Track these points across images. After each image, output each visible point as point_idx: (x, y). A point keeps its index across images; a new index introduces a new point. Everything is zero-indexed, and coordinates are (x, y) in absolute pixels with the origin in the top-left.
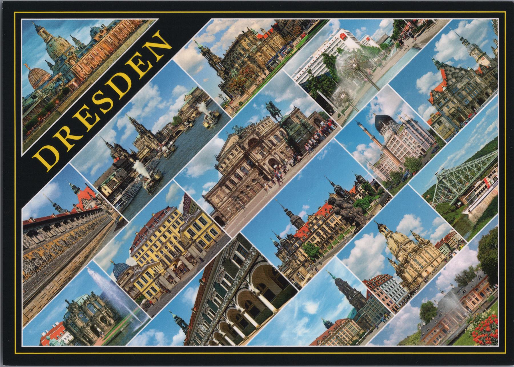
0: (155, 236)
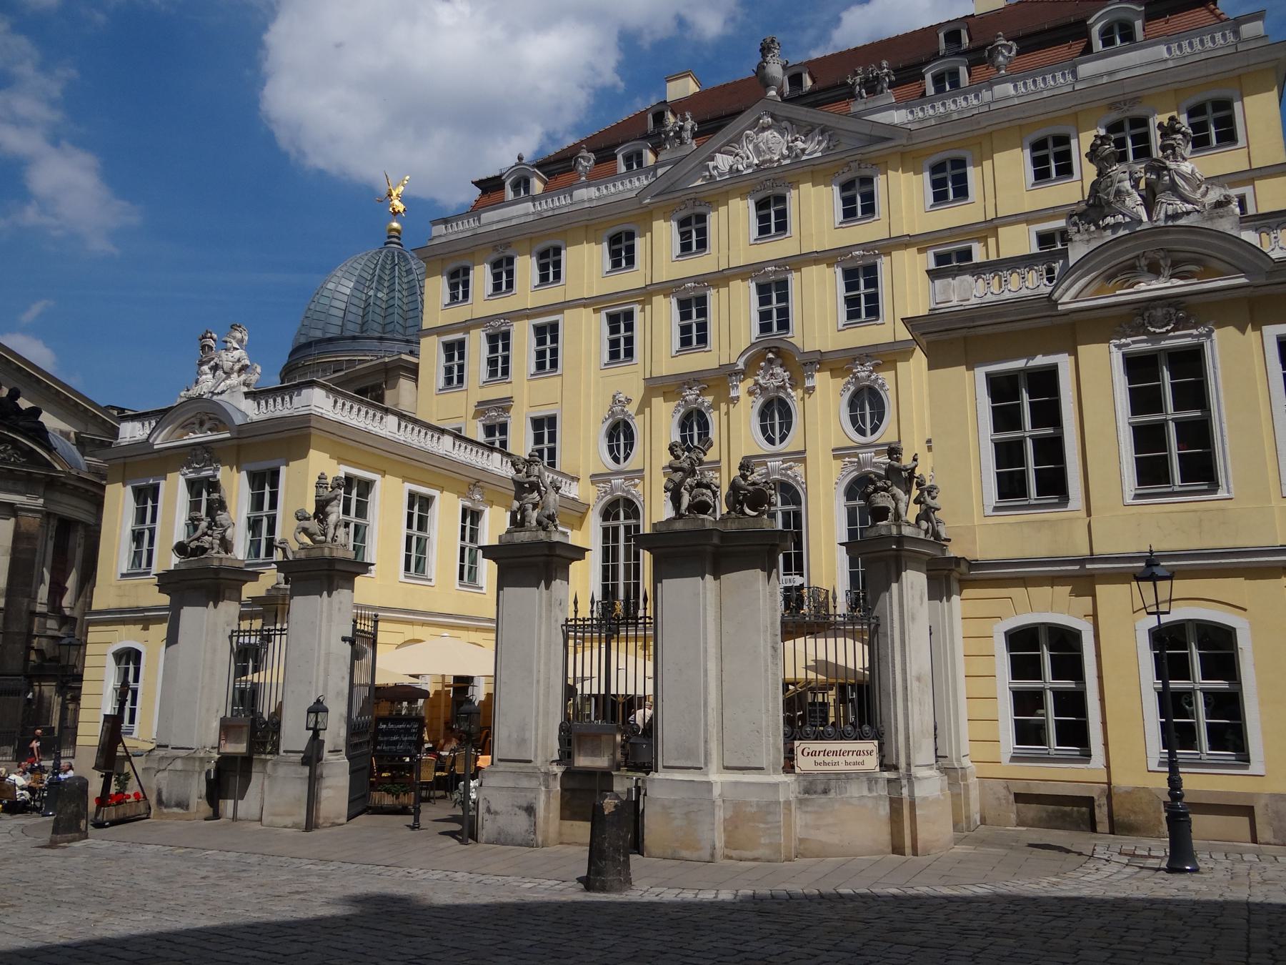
0: (772, 217)
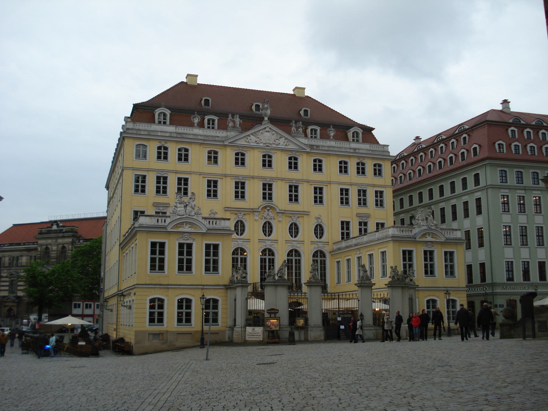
0: (267, 162)
